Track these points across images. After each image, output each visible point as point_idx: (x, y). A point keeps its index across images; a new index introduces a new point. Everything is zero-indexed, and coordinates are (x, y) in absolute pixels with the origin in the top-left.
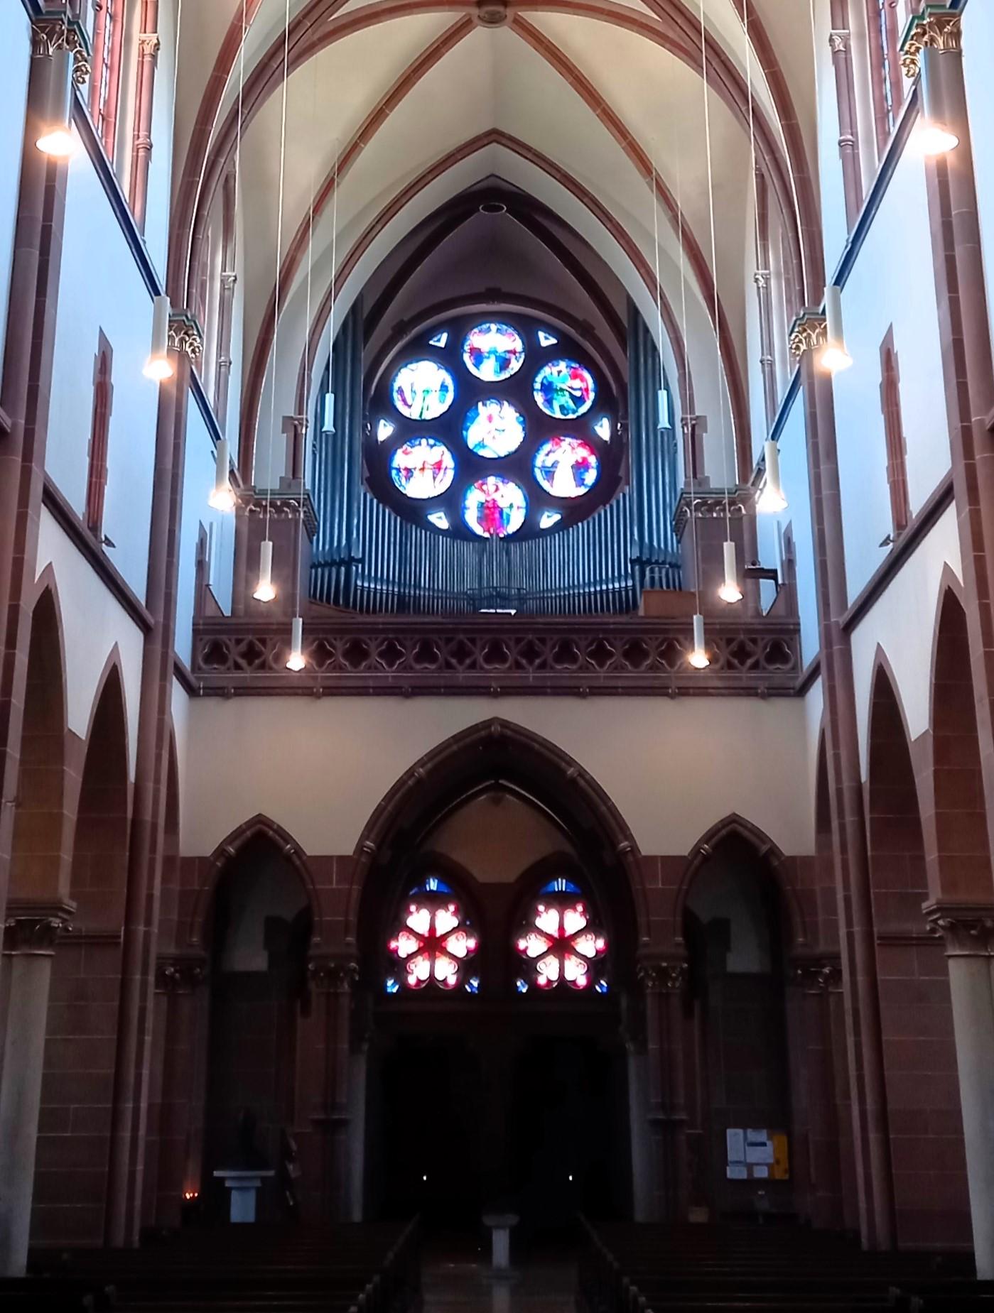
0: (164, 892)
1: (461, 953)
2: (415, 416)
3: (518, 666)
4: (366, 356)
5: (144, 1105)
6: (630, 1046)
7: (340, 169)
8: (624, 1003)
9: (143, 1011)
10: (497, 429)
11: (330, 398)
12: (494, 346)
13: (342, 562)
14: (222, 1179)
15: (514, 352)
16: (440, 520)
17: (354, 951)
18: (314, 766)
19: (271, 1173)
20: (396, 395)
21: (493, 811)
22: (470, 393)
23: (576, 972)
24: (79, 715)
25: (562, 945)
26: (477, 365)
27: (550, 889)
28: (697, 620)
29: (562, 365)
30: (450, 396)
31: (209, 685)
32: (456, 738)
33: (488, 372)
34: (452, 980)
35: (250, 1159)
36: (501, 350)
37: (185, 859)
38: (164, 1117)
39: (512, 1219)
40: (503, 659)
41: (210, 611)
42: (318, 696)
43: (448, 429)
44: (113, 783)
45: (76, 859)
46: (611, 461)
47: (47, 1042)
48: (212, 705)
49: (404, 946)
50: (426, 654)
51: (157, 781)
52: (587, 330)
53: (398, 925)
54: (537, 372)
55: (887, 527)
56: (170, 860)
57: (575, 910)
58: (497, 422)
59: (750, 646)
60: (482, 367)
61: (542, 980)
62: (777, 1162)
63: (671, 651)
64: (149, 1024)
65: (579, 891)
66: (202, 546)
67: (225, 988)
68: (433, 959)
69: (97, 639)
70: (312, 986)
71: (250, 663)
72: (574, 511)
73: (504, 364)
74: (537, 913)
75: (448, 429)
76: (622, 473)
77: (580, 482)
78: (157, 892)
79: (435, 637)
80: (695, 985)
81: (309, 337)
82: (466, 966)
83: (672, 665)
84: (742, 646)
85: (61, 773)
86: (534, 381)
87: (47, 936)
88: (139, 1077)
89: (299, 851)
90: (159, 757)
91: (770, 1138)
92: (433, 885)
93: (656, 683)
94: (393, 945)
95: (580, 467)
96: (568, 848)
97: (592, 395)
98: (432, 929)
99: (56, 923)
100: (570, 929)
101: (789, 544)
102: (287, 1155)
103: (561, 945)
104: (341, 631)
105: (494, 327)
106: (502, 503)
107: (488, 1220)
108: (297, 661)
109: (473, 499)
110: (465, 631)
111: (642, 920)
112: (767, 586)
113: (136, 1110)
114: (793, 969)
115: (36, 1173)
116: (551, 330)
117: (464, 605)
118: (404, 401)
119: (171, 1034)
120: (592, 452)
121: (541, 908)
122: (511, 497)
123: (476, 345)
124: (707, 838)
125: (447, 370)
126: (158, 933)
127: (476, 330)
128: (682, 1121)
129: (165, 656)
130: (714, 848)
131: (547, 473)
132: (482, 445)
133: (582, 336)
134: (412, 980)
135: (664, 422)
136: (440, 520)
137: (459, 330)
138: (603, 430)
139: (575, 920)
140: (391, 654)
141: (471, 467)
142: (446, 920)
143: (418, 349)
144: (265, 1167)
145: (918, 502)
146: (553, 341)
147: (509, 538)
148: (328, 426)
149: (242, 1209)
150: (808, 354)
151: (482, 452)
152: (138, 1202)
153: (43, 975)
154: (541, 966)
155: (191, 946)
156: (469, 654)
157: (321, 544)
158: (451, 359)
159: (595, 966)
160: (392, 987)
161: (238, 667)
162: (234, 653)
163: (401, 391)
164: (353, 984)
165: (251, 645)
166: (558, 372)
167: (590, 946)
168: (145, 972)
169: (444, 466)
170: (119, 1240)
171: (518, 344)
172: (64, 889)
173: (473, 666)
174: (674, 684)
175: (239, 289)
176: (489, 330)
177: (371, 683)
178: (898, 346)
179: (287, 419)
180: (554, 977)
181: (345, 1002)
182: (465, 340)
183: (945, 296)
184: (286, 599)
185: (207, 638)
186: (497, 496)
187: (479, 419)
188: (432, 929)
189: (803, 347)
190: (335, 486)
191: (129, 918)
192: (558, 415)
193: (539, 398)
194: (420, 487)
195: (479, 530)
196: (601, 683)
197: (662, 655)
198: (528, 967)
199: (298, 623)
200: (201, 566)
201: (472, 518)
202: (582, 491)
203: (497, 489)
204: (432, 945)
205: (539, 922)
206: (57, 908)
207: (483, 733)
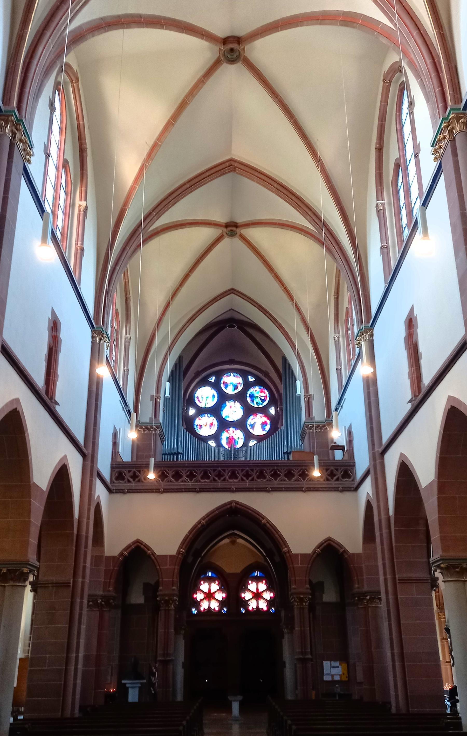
1: (220, 599)
2: (203, 406)
8: (283, 614)
10: (233, 411)
12: (232, 382)
15: (240, 383)
20: (196, 399)
22: (223, 398)
23: (263, 605)
25: (258, 596)
27: (253, 575)
29: (257, 388)
30: (216, 399)
33: (230, 391)
34: (217, 609)
36: (235, 383)
39: (240, 698)
43: (215, 411)
46: (275, 422)
49: (199, 596)
52: (266, 374)
53: (197, 589)
54: (248, 390)
57: (262, 582)
60: (227, 388)
61: (250, 608)
65: (263, 575)
73: (236, 387)
76: (279, 426)
77: (264, 429)
82: (222, 603)
86: (247, 394)
94: (195, 596)
95: (264, 424)
97: (268, 399)
98: (210, 590)
100: (261, 590)
103: (257, 596)
105: (232, 374)
106: (236, 437)
116: (253, 375)
118: (199, 401)
120: (268, 419)
121: (250, 582)
122: (238, 435)
123: (226, 381)
125: (215, 390)
127: (225, 375)
131: (251, 426)
133: (264, 376)
134: (202, 609)
136: (212, 443)
137: (219, 375)
138: (272, 411)
139: (262, 586)
141: (224, 425)
142: (215, 587)
143: (204, 382)
146: (254, 379)
151: (228, 419)
154: (250, 602)
158: (216, 386)
159: (270, 603)
160: (194, 611)
163: (198, 397)
166: (256, 391)
167: (268, 596)
169: (214, 424)
171: (240, 380)
176: (230, 375)
180: (255, 607)
182: (221, 379)
186: (233, 435)
187: (226, 407)
188: (210, 590)
192: (256, 406)
193: (249, 399)
194: (205, 432)
195: (227, 447)
198: (245, 603)
201: (224, 442)
202: (265, 433)
203: (233, 432)
204: (209, 596)
205: (249, 587)
207: (228, 506)
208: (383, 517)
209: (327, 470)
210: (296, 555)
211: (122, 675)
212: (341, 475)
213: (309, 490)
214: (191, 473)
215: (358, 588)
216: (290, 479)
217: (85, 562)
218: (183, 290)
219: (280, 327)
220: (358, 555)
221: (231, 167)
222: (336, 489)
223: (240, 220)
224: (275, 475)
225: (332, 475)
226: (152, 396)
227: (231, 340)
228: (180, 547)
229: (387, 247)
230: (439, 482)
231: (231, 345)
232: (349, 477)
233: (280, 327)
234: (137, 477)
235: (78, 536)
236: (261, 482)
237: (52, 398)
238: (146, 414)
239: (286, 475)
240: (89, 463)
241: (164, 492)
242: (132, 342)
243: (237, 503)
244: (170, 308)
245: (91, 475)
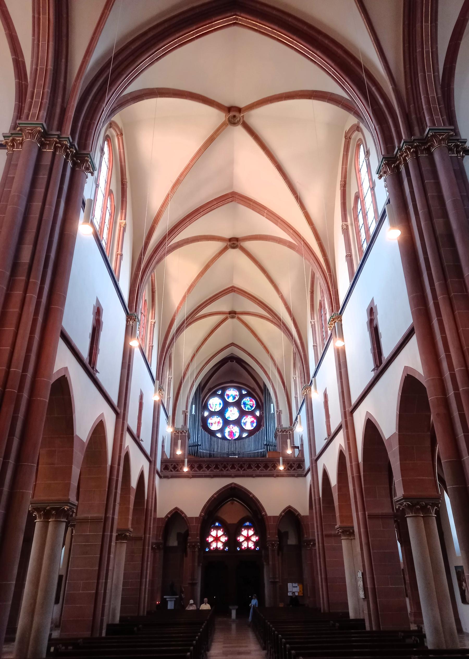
0: (153, 527)
2: (213, 411)
3: (238, 470)
4: (202, 396)
5: (148, 580)
6: (265, 563)
7: (197, 352)
8: (263, 552)
9: (148, 556)
10: (232, 414)
11: (194, 406)
12: (232, 394)
13: (196, 445)
14: (166, 598)
16: (219, 435)
17: (199, 540)
18: (189, 495)
19: (178, 597)
21: (233, 506)
22: (226, 405)
23: (251, 545)
24: (134, 483)
25: (248, 539)
26: (228, 398)
28: (281, 459)
29: (248, 398)
31: (165, 475)
32: (224, 488)
33: (230, 400)
34: (222, 548)
35: (174, 594)
37: (158, 518)
38: (152, 583)
40: (235, 468)
41: (165, 457)
42: (191, 478)
43: (221, 413)
44: (142, 500)
45: (133, 519)
46: (260, 420)
47: (125, 564)
48: (165, 480)
49: (210, 539)
50: (217, 467)
51: (152, 499)
52: (254, 390)
53: (209, 535)
55: (326, 436)
56: (155, 519)
58: (232, 412)
59: (293, 465)
62: (300, 591)
63: (275, 467)
64: (149, 560)
66: (163, 442)
67: (167, 550)
68: (217, 542)
69: (139, 464)
70: (188, 550)
71: (174, 470)
72: (251, 433)
73: (234, 398)
74: (242, 531)
75: (221, 413)
76: (262, 424)
77: (252, 426)
78: (152, 526)
79: (219, 463)
80: (280, 548)
81: (189, 392)
82: (225, 544)
83: (275, 469)
84: (291, 464)
85: (130, 497)
87: (125, 538)
88: (147, 573)
89: (186, 516)
90: (152, 493)
91: (298, 585)
92: (217, 524)
93: (271, 474)
95: (252, 422)
96: (250, 515)
98: (217, 535)
99: (128, 534)
100: (250, 535)
101: (302, 440)
102: (182, 592)
103: (248, 539)
104: (196, 462)
106: (234, 431)
107: (231, 607)
108: (186, 469)
109: (227, 430)
110: (226, 462)
111: (268, 532)
112: (297, 450)
113: (146, 581)
114: (303, 544)
115: (122, 598)
117: (225, 456)
119: (154, 562)
122: (236, 430)
124: (284, 511)
126: (152, 537)
128: (277, 582)
129: (154, 468)
130: (285, 514)
132: (229, 417)
135: (272, 412)
137: (224, 390)
138: (258, 413)
139: (251, 532)
140: (208, 467)
141: (227, 422)
142: (220, 533)
143: (214, 394)
144: (177, 595)
145: (333, 430)
146: (246, 393)
147: (235, 440)
148: (193, 413)
149: (171, 606)
150: (306, 395)
152: (146, 604)
153: (125, 546)
154: (243, 544)
155: (159, 540)
156: (227, 467)
157: (191, 442)
158: (222, 396)
159: (256, 544)
161: (171, 471)
162: (171, 468)
163: (210, 404)
164: (199, 549)
165: (175, 466)
166: (247, 400)
167: (254, 539)
168: (149, 546)
170: (141, 614)
171: (238, 393)
172: (130, 526)
173: (228, 470)
174: (275, 474)
175: (172, 380)
177: (203, 475)
178: (328, 393)
179: (184, 411)
180: (246, 546)
181: (197, 554)
183: (340, 381)
184: (184, 455)
185: (164, 464)
186: (232, 430)
188: (217, 535)
189: (305, 393)
190: (194, 428)
191: (145, 533)
193: (242, 406)
195: (228, 438)
196: (258, 474)
197: (272, 467)
198: (240, 544)
199: (186, 460)
200: (163, 446)
201: (227, 435)
202: (253, 428)
204: (217, 539)
206: (128, 530)
208: (317, 498)
209: (288, 464)
210: (270, 517)
211: (164, 593)
212: (296, 467)
213: (278, 476)
214: (208, 466)
215: (306, 537)
216: (266, 469)
217: (150, 525)
218: (203, 347)
219: (262, 367)
220: (306, 517)
221: (233, 289)
222: (293, 476)
223: (238, 310)
224: (258, 467)
225: (291, 467)
226: (184, 411)
227: (230, 370)
228: (201, 512)
229: (316, 346)
230: (338, 486)
231: (232, 371)
232: (301, 468)
233: (262, 367)
234: (176, 468)
235: (146, 509)
236: (249, 471)
237: (139, 436)
238: (180, 423)
239: (264, 467)
240: (153, 466)
241: (192, 477)
242: (172, 380)
243: (235, 484)
244: (195, 358)
245: (154, 474)
